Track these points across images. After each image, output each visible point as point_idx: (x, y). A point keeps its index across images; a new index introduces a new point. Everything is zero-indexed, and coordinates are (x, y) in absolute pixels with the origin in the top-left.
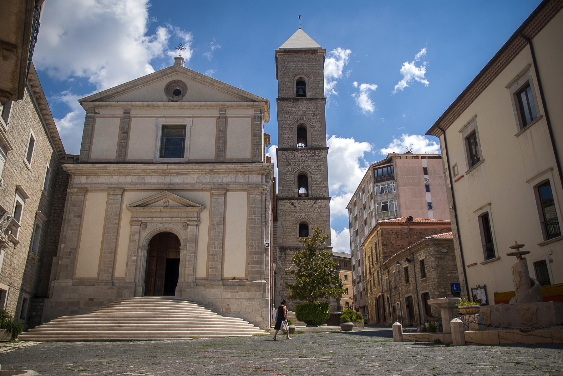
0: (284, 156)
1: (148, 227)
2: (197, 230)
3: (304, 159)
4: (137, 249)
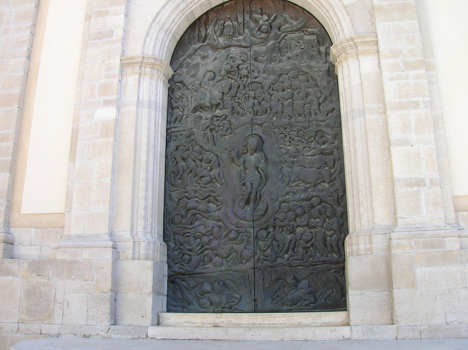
4: (117, 71)
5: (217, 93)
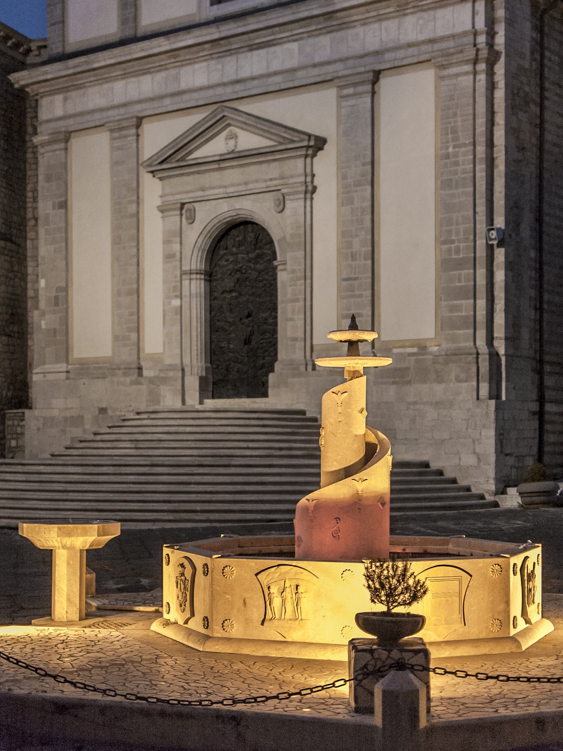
1: (199, 216)
2: (308, 209)
4: (179, 279)
5: (232, 284)
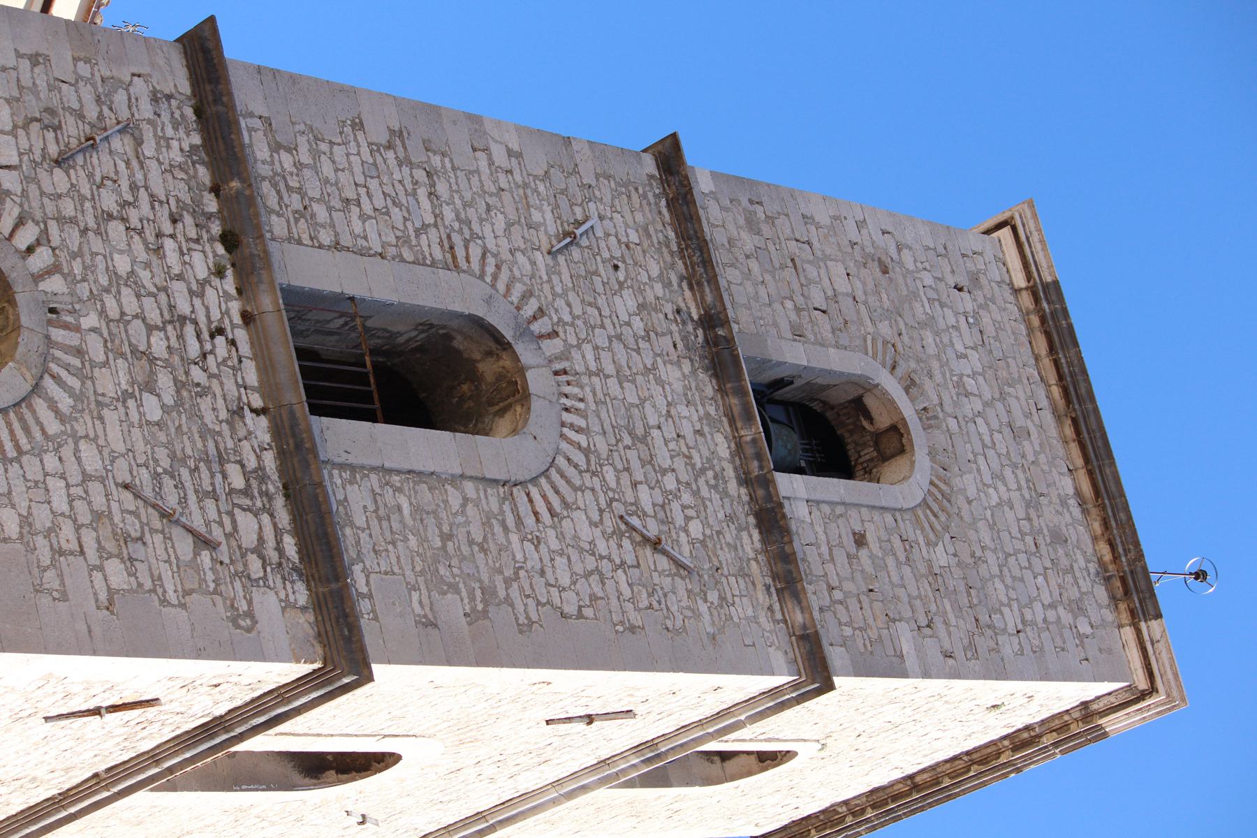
0: (145, 109)
3: (158, 345)
